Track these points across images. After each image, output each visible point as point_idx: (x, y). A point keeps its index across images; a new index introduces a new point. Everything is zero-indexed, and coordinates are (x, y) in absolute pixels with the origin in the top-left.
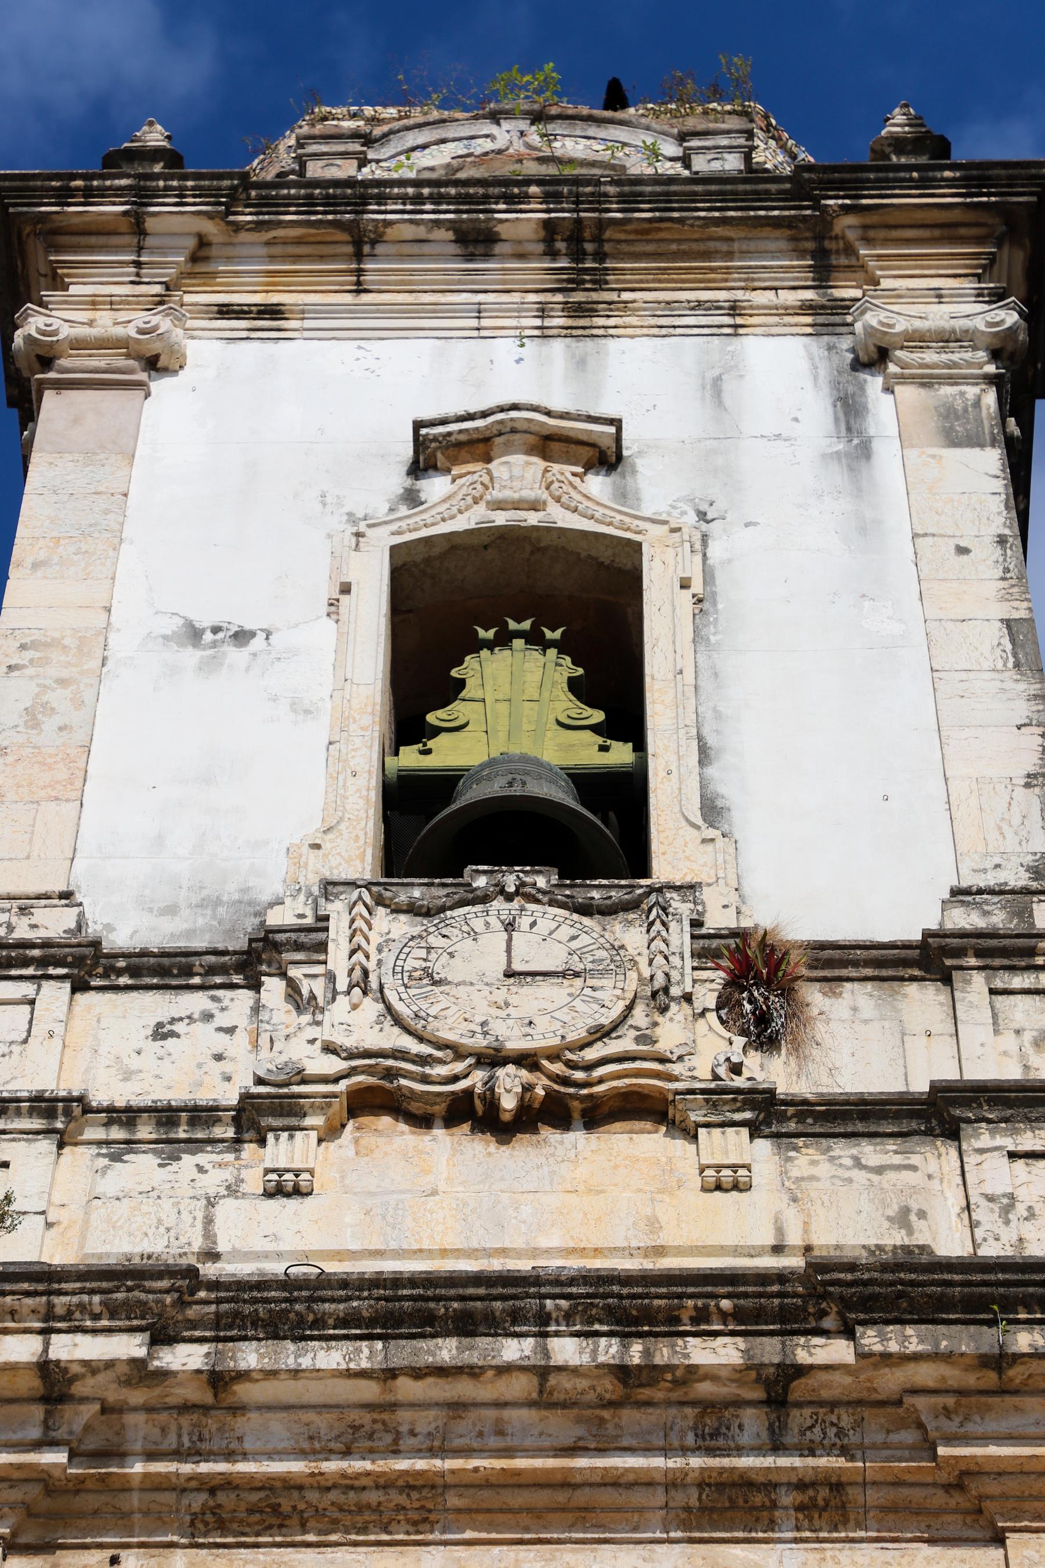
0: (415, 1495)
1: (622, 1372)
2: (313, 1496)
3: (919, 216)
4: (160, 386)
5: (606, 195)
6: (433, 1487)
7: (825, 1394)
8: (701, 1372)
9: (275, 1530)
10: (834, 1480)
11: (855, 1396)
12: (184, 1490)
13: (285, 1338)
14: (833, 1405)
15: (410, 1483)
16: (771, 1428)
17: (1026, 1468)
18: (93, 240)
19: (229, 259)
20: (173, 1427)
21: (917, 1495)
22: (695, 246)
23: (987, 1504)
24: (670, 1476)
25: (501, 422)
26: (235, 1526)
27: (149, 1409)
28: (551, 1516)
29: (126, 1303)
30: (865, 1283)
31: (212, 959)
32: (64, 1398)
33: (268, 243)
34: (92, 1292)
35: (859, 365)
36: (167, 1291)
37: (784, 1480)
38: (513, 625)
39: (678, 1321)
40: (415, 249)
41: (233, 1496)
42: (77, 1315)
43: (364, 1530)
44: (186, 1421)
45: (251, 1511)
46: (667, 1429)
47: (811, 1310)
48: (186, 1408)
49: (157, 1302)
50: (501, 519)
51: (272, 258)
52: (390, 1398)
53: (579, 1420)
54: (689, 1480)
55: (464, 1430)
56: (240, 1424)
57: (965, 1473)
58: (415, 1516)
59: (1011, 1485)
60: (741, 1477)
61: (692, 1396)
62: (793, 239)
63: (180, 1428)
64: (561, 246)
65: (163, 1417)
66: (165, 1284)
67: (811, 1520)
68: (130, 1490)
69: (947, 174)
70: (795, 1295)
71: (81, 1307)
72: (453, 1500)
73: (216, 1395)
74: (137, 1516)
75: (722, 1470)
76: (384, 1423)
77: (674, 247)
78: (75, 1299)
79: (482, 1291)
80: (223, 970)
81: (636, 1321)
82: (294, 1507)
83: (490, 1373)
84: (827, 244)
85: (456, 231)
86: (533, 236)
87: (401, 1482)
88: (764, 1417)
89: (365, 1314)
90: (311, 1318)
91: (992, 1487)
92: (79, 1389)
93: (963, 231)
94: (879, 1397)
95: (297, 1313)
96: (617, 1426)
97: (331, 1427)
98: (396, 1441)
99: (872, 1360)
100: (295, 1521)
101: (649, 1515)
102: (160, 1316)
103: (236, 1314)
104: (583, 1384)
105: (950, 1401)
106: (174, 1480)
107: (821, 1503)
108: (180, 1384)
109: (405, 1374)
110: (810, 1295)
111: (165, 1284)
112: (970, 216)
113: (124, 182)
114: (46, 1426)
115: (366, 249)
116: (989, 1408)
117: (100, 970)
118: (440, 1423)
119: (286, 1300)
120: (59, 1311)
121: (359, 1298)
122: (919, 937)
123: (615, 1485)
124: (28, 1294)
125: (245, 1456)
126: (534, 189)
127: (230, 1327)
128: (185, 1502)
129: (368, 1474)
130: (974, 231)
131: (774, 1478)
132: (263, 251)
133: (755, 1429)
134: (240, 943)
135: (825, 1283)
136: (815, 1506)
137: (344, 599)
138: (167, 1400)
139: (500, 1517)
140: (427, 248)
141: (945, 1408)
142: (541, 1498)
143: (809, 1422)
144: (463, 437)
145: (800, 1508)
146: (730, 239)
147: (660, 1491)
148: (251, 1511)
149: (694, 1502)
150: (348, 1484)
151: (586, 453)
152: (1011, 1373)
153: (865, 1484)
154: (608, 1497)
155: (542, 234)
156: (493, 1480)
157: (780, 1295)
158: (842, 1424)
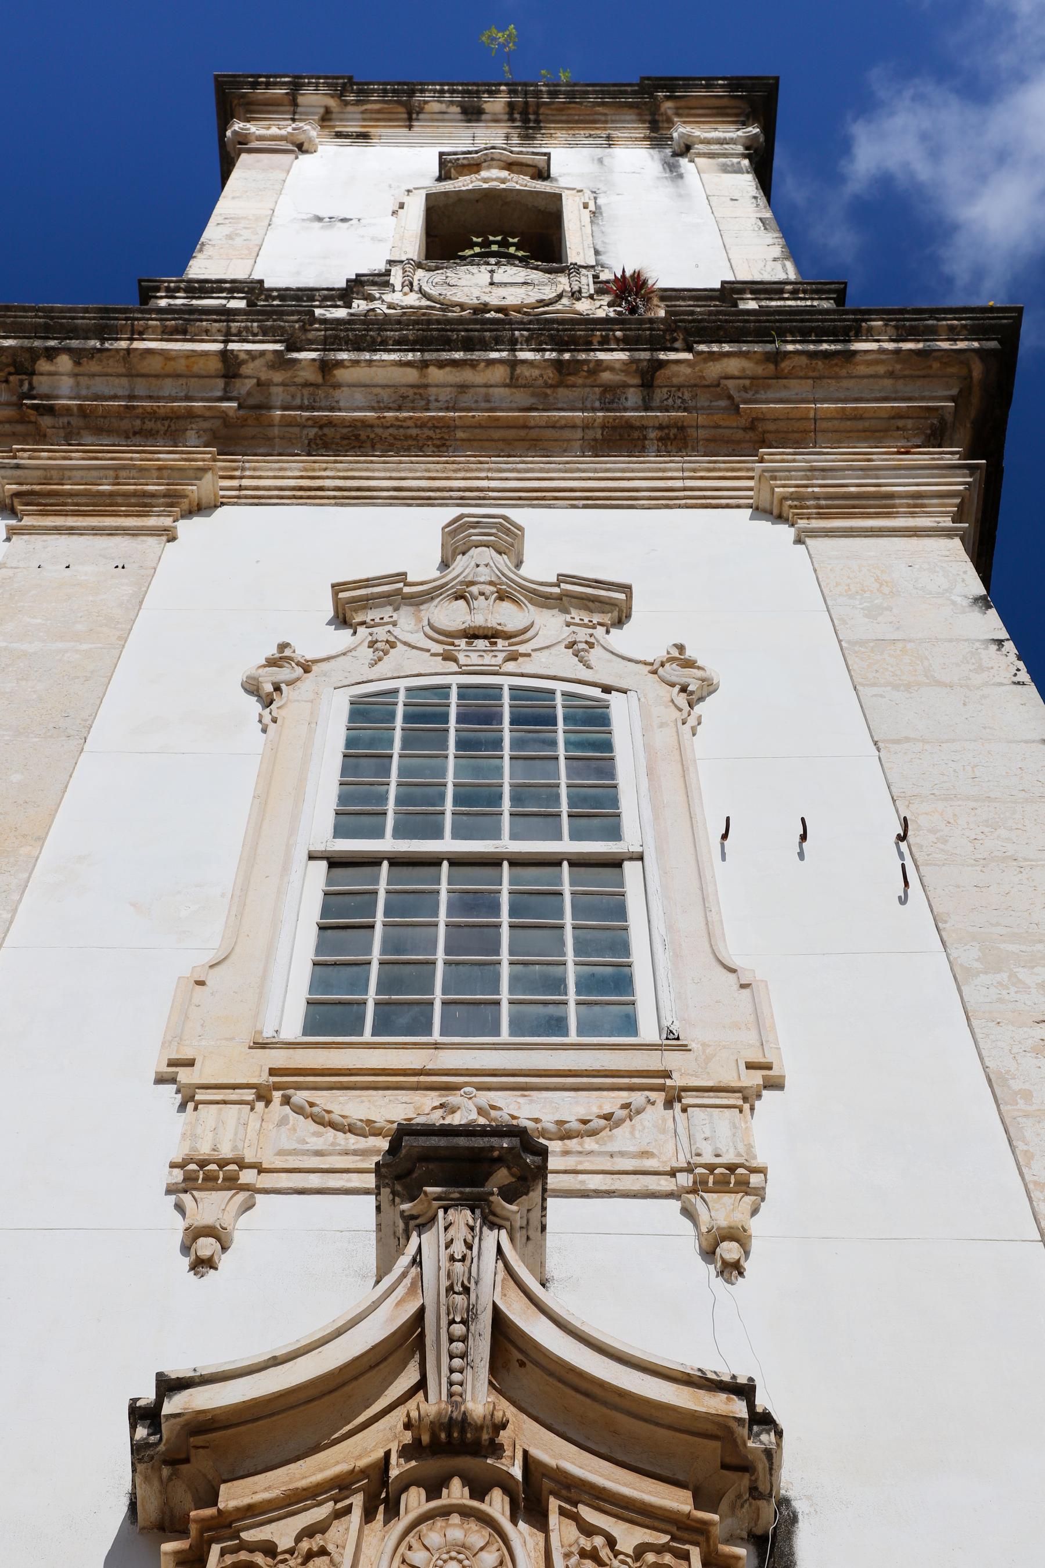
0: (438, 431)
1: (558, 364)
2: (379, 431)
3: (706, 102)
4: (303, 157)
5: (541, 91)
6: (448, 427)
7: (675, 381)
8: (604, 365)
9: (357, 449)
10: (680, 424)
11: (692, 382)
12: (305, 426)
13: (364, 350)
14: (679, 387)
15: (436, 425)
16: (644, 399)
17: (791, 416)
18: (270, 108)
19: (341, 120)
20: (299, 395)
21: (727, 433)
22: (587, 118)
23: (767, 435)
24: (585, 421)
25: (486, 154)
26: (334, 446)
27: (283, 384)
28: (516, 443)
29: (272, 327)
30: (700, 321)
31: (326, 292)
32: (237, 376)
33: (362, 113)
34: (253, 321)
35: (675, 154)
36: (297, 322)
37: (651, 424)
38: (491, 238)
39: (591, 343)
40: (440, 116)
41: (333, 430)
42: (244, 333)
43: (408, 449)
44: (306, 392)
45: (343, 438)
46: (584, 400)
47: (668, 337)
48: (306, 384)
49: (290, 327)
50: (485, 186)
51: (364, 120)
52: (424, 381)
53: (533, 395)
54: (596, 424)
55: (466, 399)
56: (337, 394)
57: (754, 420)
58: (438, 443)
59: (782, 425)
60: (626, 422)
61: (598, 382)
62: (639, 114)
63: (303, 395)
64: (517, 116)
65: (293, 389)
66: (295, 318)
67: (666, 446)
68: (273, 426)
69: (720, 82)
70: (659, 330)
71: (246, 328)
72: (460, 434)
73: (324, 377)
74: (277, 440)
75: (615, 418)
76: (421, 395)
77: (576, 118)
78: (243, 324)
79: (478, 327)
80: (331, 298)
81: (567, 343)
82: (368, 437)
83: (483, 364)
84: (657, 117)
85: (462, 107)
86: (502, 111)
87: (430, 424)
88: (640, 393)
89: (411, 338)
90: (379, 339)
91: (771, 427)
92: (246, 370)
93: (729, 111)
94: (706, 383)
95: (371, 337)
96: (555, 398)
97: (390, 397)
98: (428, 404)
99: (703, 356)
100: (368, 444)
101: (573, 443)
102: (292, 335)
103: (336, 337)
104: (536, 372)
105: (747, 382)
106: (299, 419)
107: (672, 436)
108: (303, 369)
109: (434, 365)
110: (667, 330)
111: (295, 318)
112: (733, 103)
113: (287, 79)
114: (225, 390)
115: (414, 116)
116: (769, 387)
117: (263, 297)
118: (453, 396)
119: (365, 330)
120: (234, 331)
121: (407, 330)
122: (718, 286)
123: (553, 427)
124: (215, 321)
125: (340, 410)
126: (503, 88)
127: (333, 344)
128: (305, 432)
129: (411, 418)
130: (734, 111)
131: (645, 423)
132: (360, 116)
133: (634, 400)
134: (343, 285)
135: (676, 322)
136: (669, 439)
137: (400, 211)
138: (296, 380)
139: (487, 444)
140: (446, 116)
141: (744, 387)
142: (511, 434)
143: (666, 396)
144: (465, 162)
145: (660, 439)
146: (605, 114)
147: (579, 431)
148: (343, 438)
149: (599, 436)
150: (398, 424)
151: (531, 170)
152: (783, 365)
153: (697, 427)
154: (549, 433)
155: (507, 109)
156: (483, 423)
157: (650, 329)
158: (685, 397)
